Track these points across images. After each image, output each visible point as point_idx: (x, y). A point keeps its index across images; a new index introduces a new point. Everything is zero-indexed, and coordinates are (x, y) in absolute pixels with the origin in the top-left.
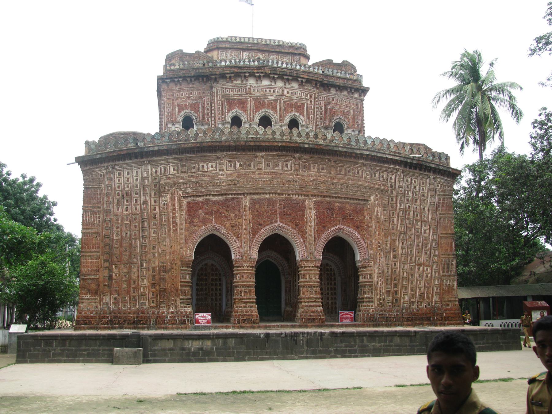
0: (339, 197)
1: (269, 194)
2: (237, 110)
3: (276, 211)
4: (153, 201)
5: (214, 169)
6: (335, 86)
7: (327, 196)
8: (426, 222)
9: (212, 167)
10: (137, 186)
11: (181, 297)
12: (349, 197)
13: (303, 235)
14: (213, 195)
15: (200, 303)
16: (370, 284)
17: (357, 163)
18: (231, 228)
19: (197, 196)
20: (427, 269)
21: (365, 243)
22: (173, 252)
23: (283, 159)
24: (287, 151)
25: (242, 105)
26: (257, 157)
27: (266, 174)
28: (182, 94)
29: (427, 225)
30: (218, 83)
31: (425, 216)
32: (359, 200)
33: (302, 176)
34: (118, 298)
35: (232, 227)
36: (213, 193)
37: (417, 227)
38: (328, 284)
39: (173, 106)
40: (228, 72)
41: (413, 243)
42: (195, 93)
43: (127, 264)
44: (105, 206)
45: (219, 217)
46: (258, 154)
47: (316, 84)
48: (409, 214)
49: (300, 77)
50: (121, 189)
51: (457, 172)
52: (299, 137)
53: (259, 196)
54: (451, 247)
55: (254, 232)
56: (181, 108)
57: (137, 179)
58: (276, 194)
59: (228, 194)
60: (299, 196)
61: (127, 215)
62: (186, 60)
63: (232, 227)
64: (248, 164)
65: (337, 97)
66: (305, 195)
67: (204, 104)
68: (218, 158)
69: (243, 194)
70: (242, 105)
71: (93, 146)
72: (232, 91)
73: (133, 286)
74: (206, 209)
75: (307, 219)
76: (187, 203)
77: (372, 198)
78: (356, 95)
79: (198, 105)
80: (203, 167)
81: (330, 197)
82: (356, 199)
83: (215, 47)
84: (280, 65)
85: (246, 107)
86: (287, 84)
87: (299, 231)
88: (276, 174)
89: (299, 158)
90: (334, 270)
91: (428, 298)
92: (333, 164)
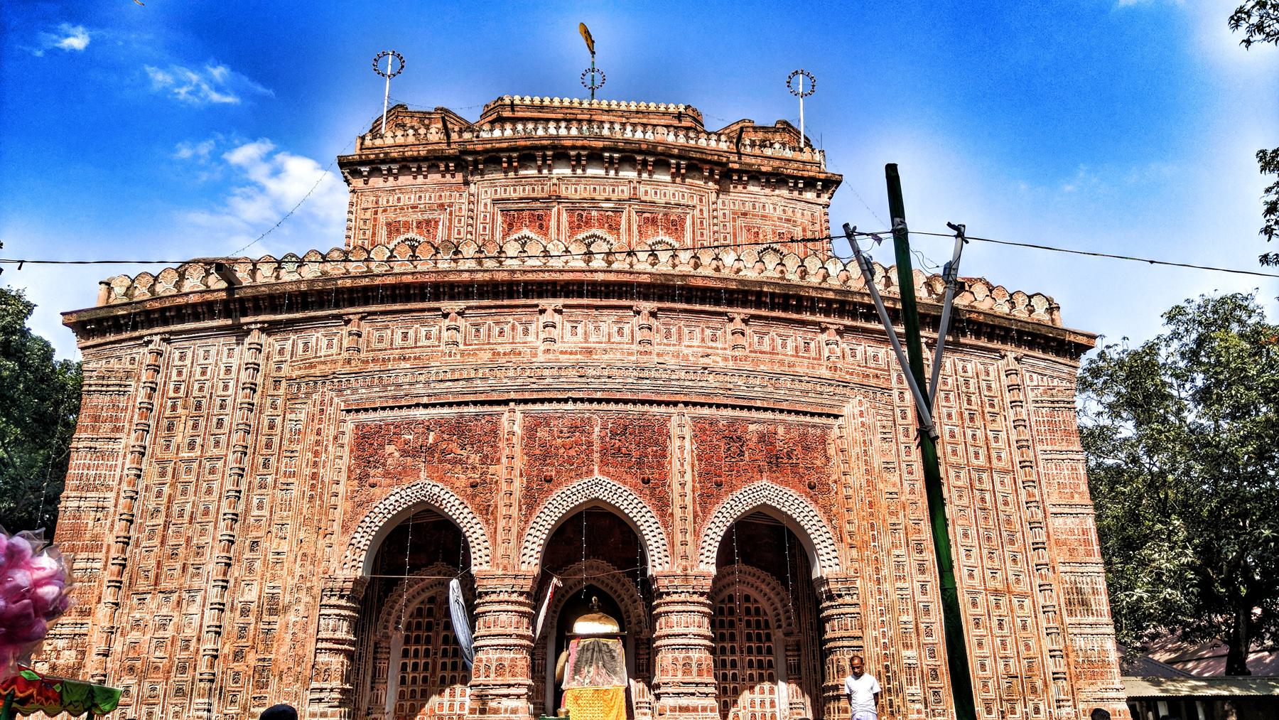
0: (758, 409)
1: (575, 401)
2: (526, 232)
3: (590, 444)
4: (266, 423)
5: (433, 342)
6: (755, 176)
7: (726, 406)
8: (1006, 472)
9: (428, 337)
10: (226, 388)
11: (314, 685)
12: (785, 406)
13: (662, 505)
14: (426, 406)
15: (407, 704)
16: (855, 643)
17: (803, 323)
18: (469, 490)
19: (384, 409)
20: (1021, 607)
21: (835, 528)
22: (304, 555)
23: (612, 316)
24: (620, 298)
25: (540, 223)
26: (542, 312)
27: (566, 353)
28: (399, 199)
29: (1008, 479)
30: (482, 173)
31: (999, 458)
32: (813, 415)
33: (658, 355)
34: (134, 690)
35: (474, 486)
36: (425, 400)
37: (977, 485)
38: (750, 650)
39: (375, 226)
40: (505, 145)
41: (972, 532)
42: (430, 198)
43: (171, 592)
44: (133, 435)
45: (440, 462)
46: (543, 302)
47: (712, 172)
48: (954, 453)
49: (673, 156)
50: (182, 394)
51: (1083, 340)
52: (653, 265)
53: (546, 406)
54: (1087, 542)
55: (531, 501)
56: (393, 229)
57: (228, 370)
58: (591, 401)
59: (466, 404)
60: (651, 403)
61: (191, 460)
62: (412, 127)
63: (474, 486)
64: (520, 328)
65: (763, 199)
66: (667, 404)
67: (450, 220)
68: (446, 316)
69: (506, 402)
70: (540, 223)
71: (119, 290)
72: (515, 191)
73: (184, 655)
74: (407, 442)
75: (676, 465)
76: (357, 427)
77: (850, 408)
78: (810, 195)
79: (436, 222)
80: (405, 336)
81: (734, 407)
82: (805, 414)
83: (494, 116)
84: (628, 134)
85: (548, 228)
86: (645, 176)
87: (652, 495)
88: (589, 352)
89: (653, 314)
90: (765, 613)
91: (1034, 690)
92: (738, 325)
